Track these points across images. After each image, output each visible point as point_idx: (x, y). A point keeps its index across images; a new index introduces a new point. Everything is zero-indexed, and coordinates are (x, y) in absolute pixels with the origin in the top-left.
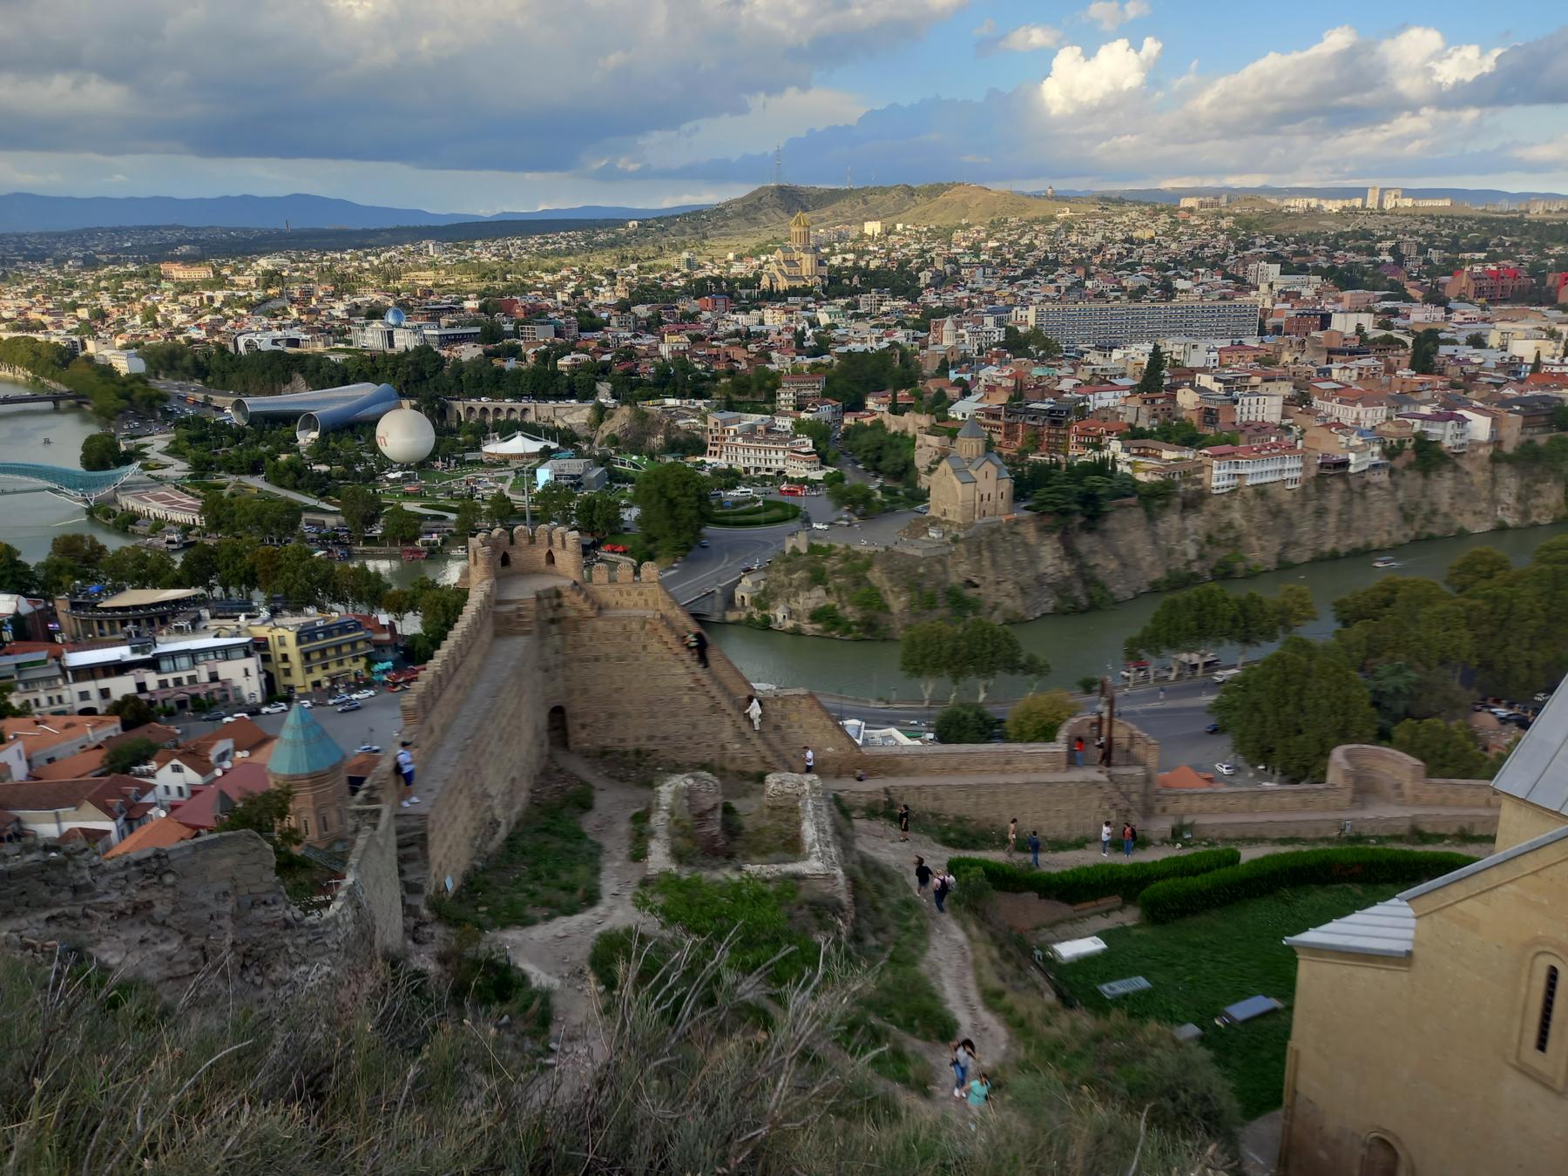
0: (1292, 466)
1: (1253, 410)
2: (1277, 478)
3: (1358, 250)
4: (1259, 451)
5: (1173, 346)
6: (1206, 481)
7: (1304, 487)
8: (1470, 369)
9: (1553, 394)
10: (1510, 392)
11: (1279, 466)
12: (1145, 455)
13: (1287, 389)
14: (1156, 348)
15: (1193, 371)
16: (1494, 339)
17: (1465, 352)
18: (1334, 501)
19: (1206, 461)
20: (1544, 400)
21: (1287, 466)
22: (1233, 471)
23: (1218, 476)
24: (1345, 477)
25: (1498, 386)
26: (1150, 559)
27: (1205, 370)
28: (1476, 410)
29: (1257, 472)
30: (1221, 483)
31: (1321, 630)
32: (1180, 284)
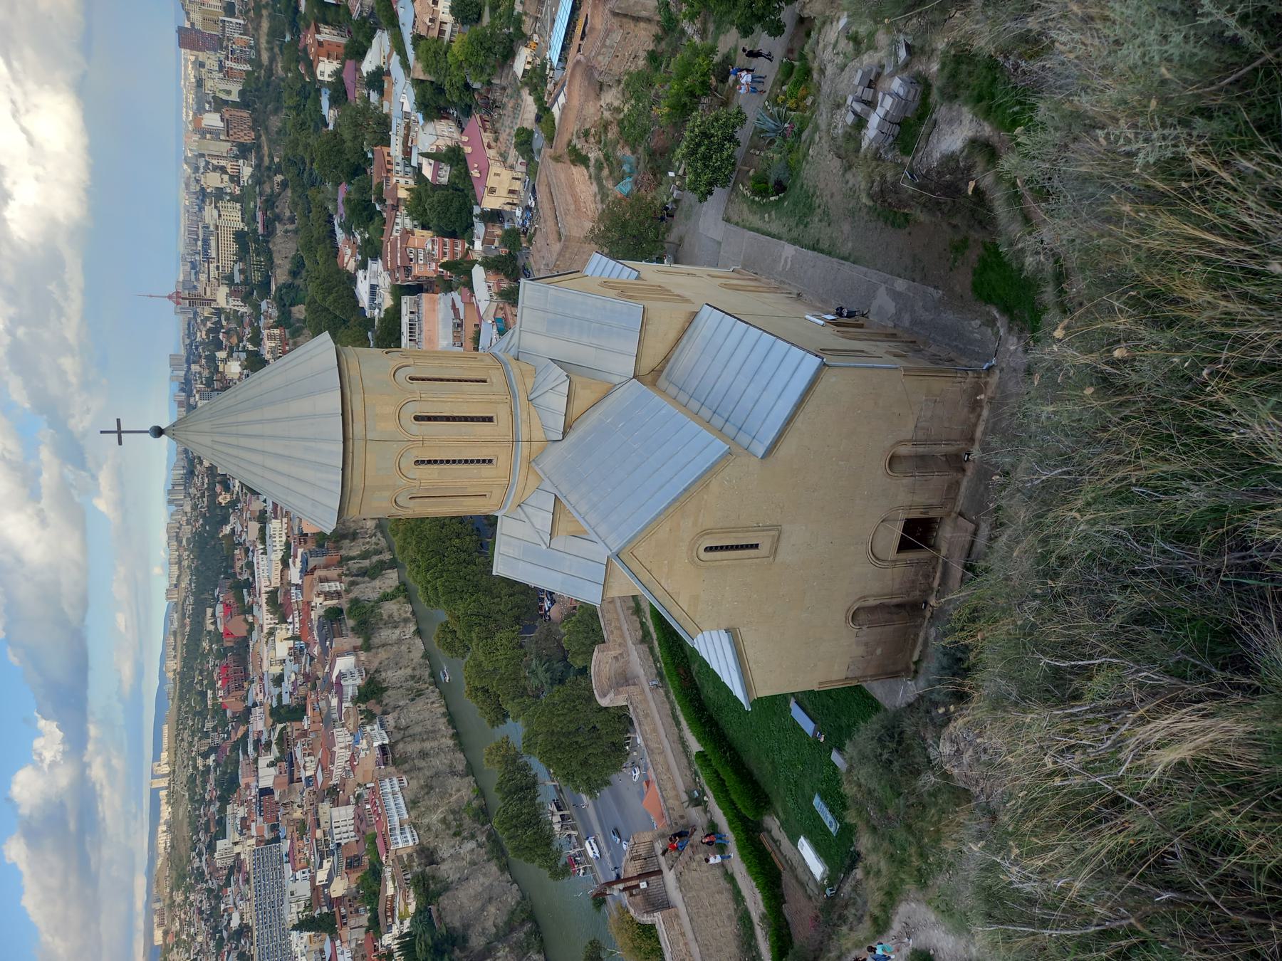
0: (389, 786)
1: (344, 829)
2: (400, 795)
3: (205, 782)
4: (379, 815)
5: (292, 913)
6: (409, 851)
7: (405, 772)
8: (301, 679)
9: (315, 623)
10: (316, 650)
11: (390, 796)
12: (393, 910)
13: (325, 807)
14: (295, 928)
15: (314, 889)
16: (276, 670)
17: (287, 686)
18: (412, 748)
19: (392, 855)
20: (321, 627)
21: (389, 790)
22: (398, 831)
23: (404, 842)
24: (393, 745)
25: (312, 659)
26: (482, 879)
27: (313, 879)
28: (331, 669)
29: (397, 810)
30: (409, 838)
31: (515, 730)
32: (235, 923)
